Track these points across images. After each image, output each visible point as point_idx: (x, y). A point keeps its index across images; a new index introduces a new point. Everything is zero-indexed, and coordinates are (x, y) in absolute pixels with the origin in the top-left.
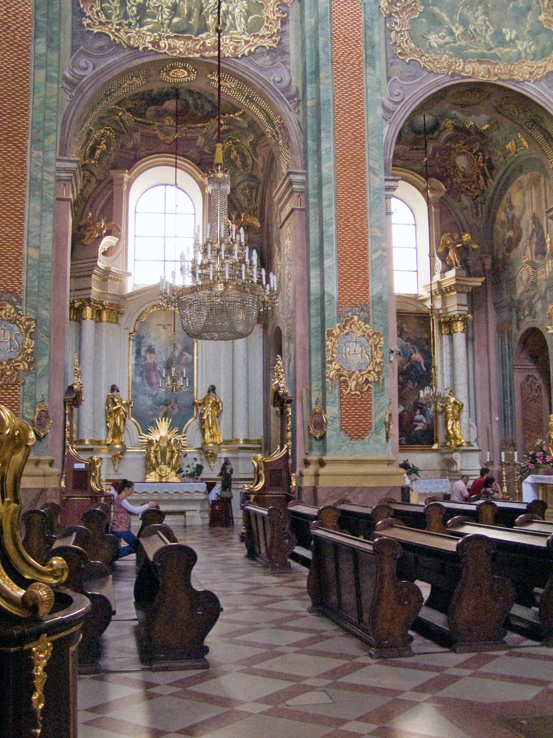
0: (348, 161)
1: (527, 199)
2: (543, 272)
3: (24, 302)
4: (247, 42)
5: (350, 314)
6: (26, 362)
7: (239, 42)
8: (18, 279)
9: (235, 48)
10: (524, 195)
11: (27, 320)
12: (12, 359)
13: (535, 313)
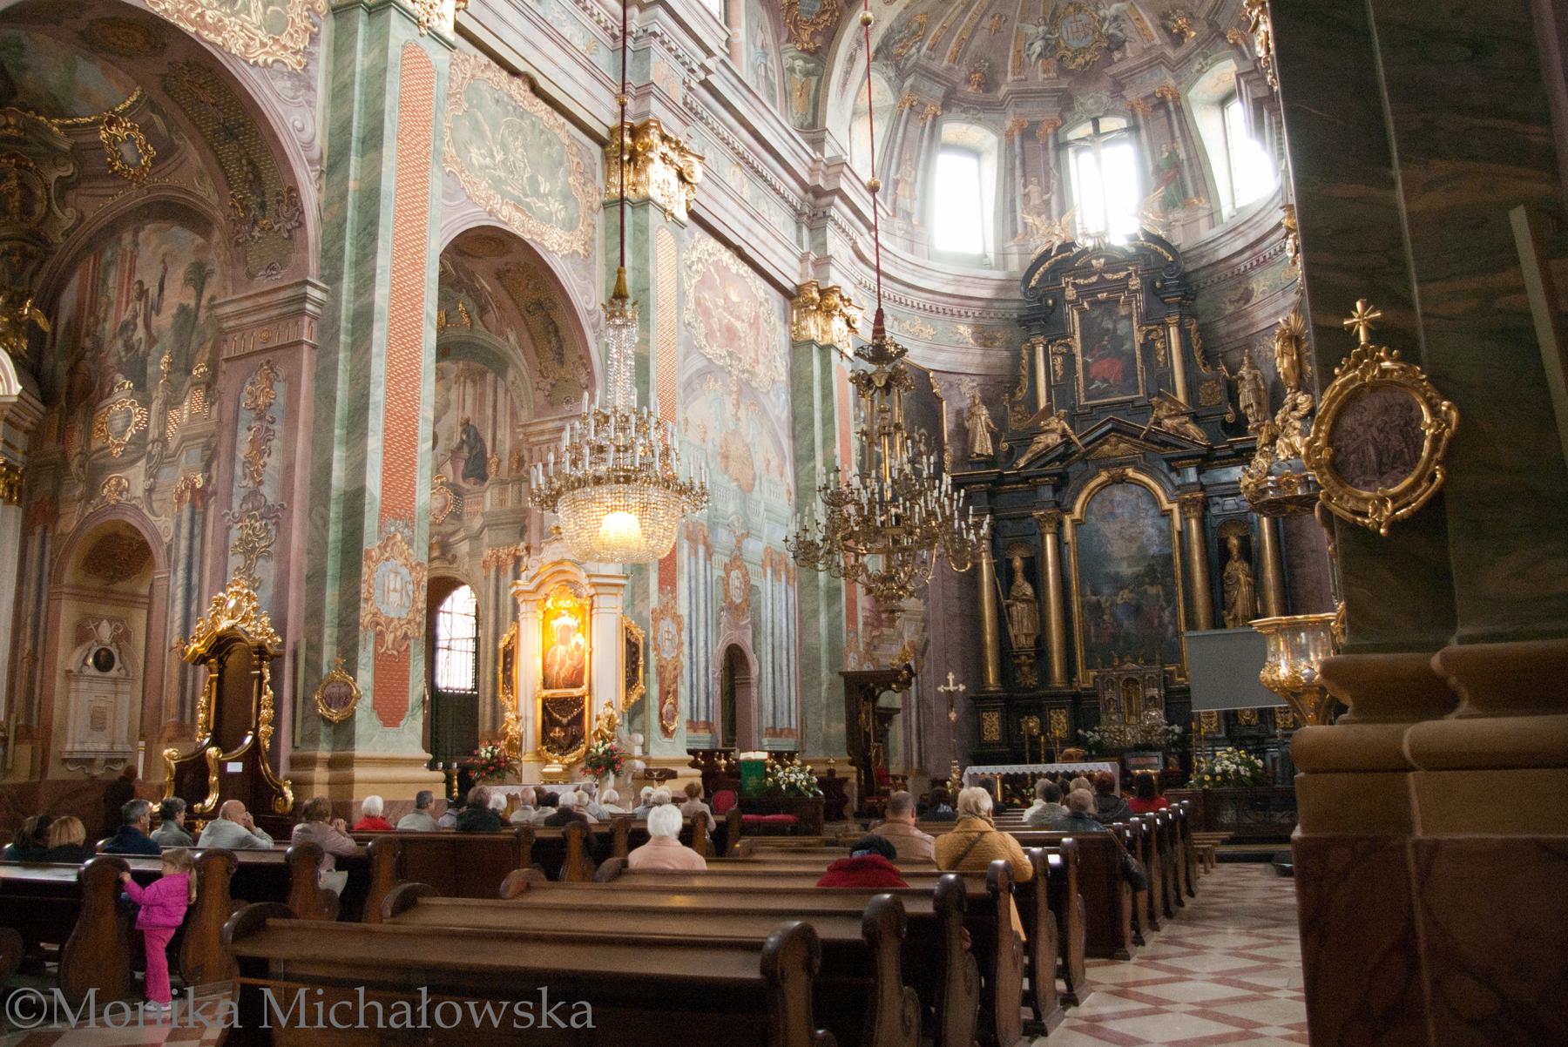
0: (405, 294)
1: (453, 396)
2: (478, 503)
4: (263, 45)
5: (393, 529)
7: (252, 39)
9: (247, 46)
10: (448, 390)
13: (455, 557)
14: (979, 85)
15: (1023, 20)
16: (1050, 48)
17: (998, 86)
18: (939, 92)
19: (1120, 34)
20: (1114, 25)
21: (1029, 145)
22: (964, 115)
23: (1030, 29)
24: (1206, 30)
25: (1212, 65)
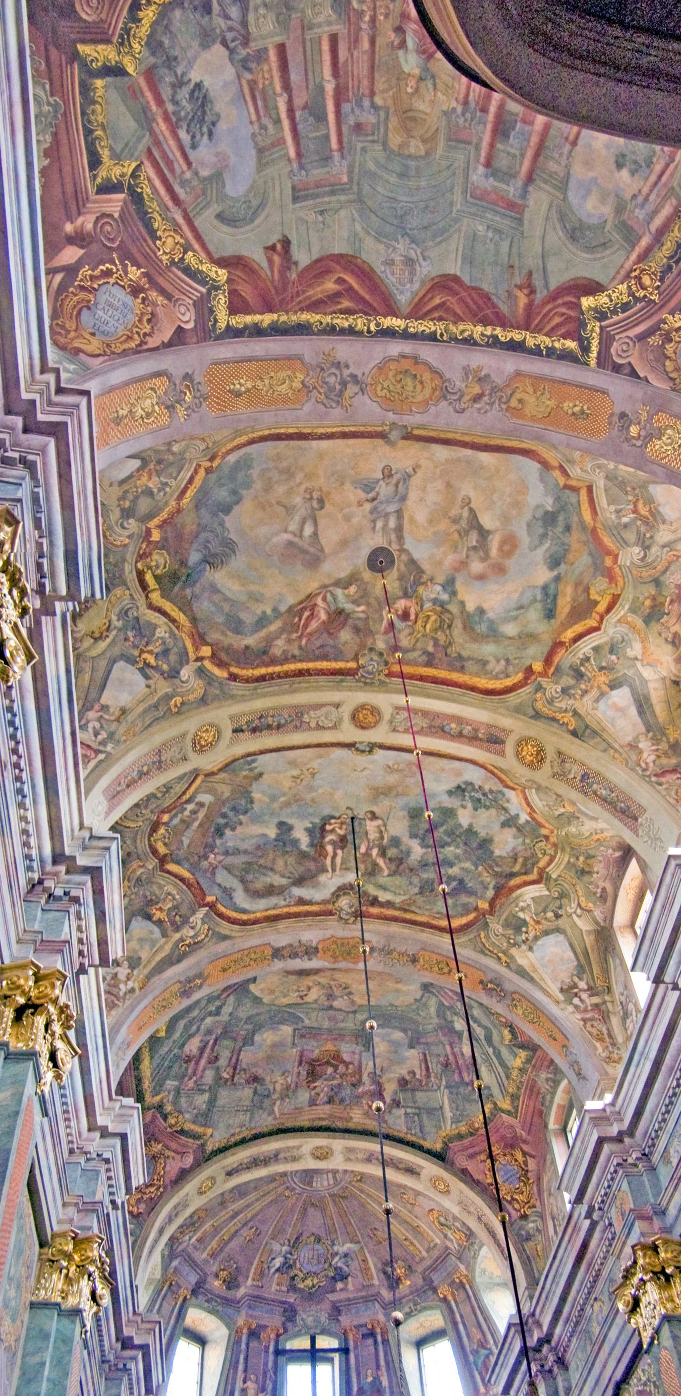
14: (224, 1281)
15: (274, 1237)
16: (287, 1266)
17: (238, 1286)
18: (193, 1279)
19: (346, 1269)
20: (343, 1260)
21: (254, 1344)
22: (206, 1305)
23: (276, 1247)
24: (420, 1282)
25: (420, 1311)
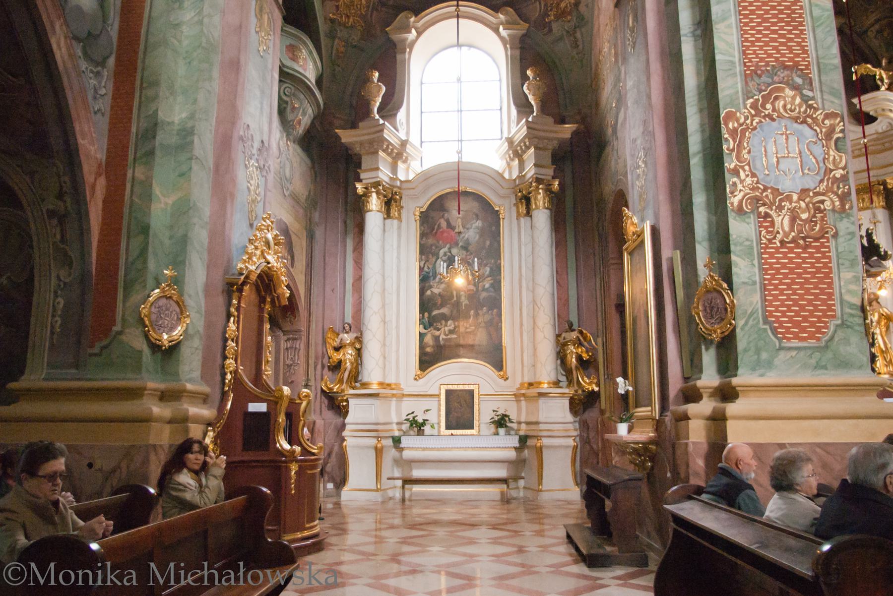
3: (816, 83)
6: (836, 194)
8: (799, 44)
11: (827, 116)
12: (808, 190)
